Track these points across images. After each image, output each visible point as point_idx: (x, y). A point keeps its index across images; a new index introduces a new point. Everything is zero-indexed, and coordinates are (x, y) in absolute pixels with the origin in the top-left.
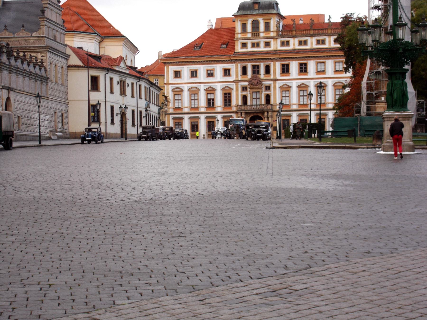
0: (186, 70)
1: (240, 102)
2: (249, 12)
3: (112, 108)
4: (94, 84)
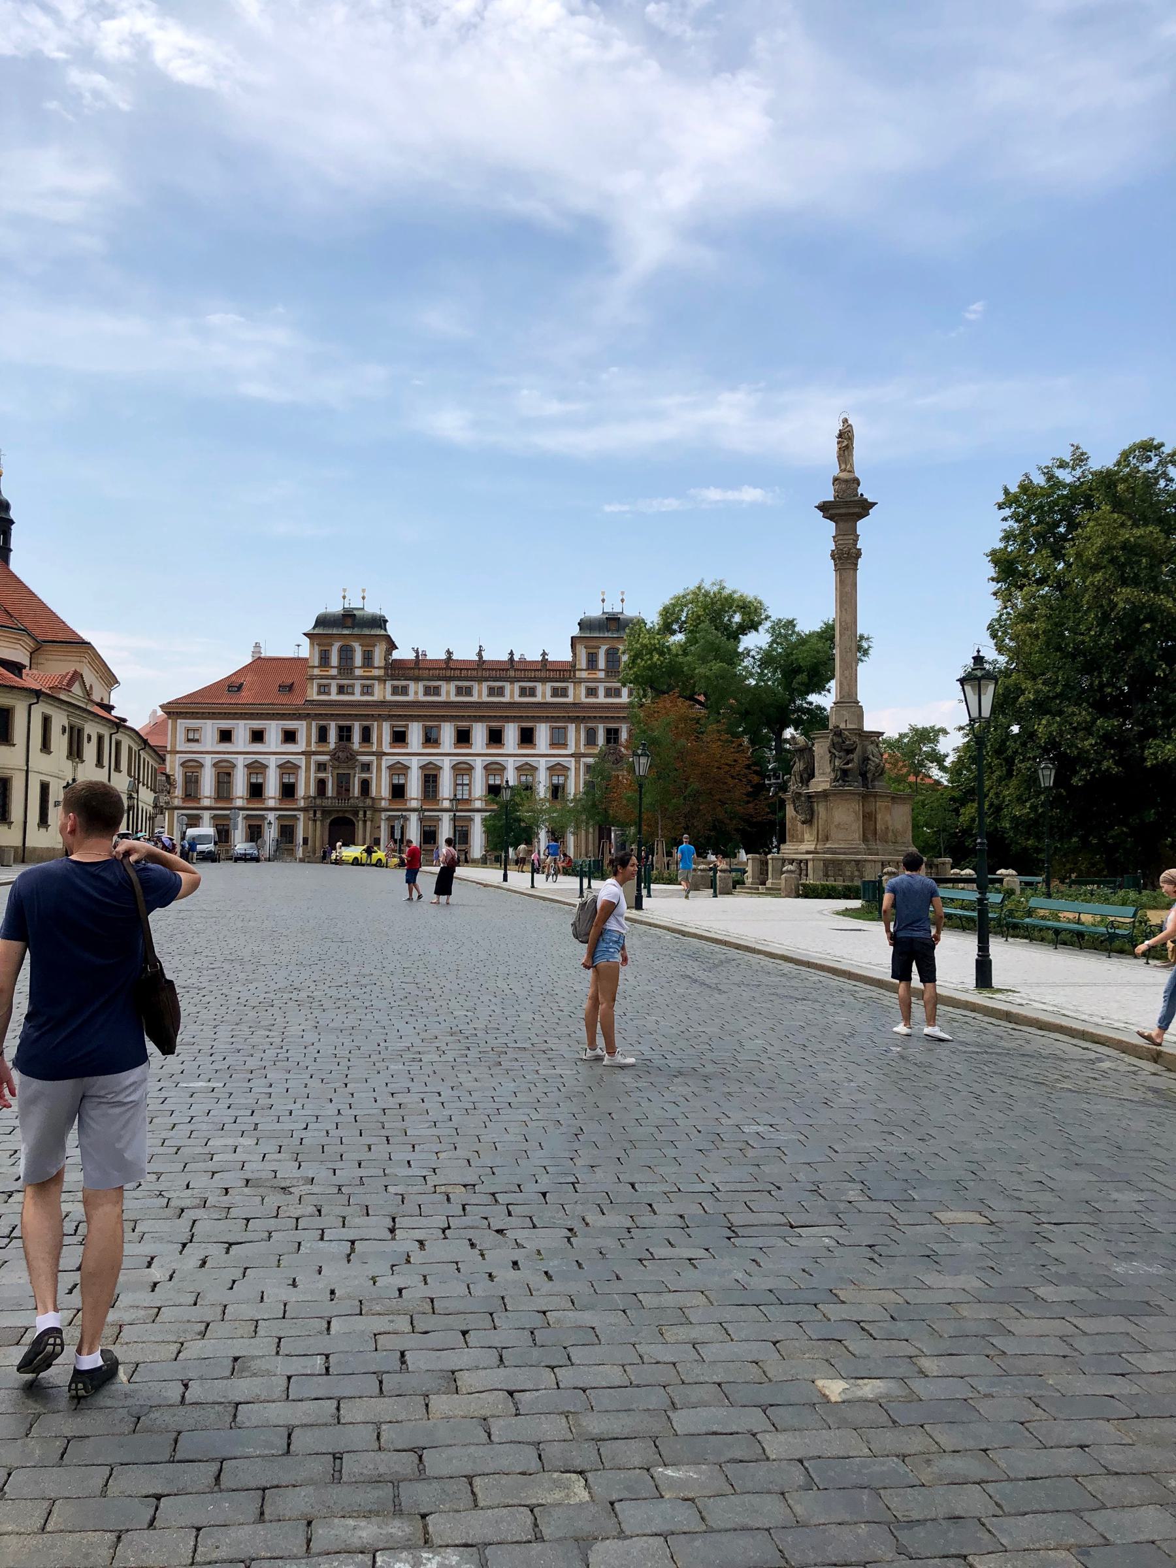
0: (209, 729)
1: (312, 792)
2: (335, 631)
3: (45, 788)
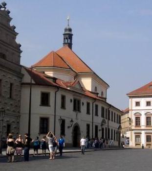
4: (45, 100)
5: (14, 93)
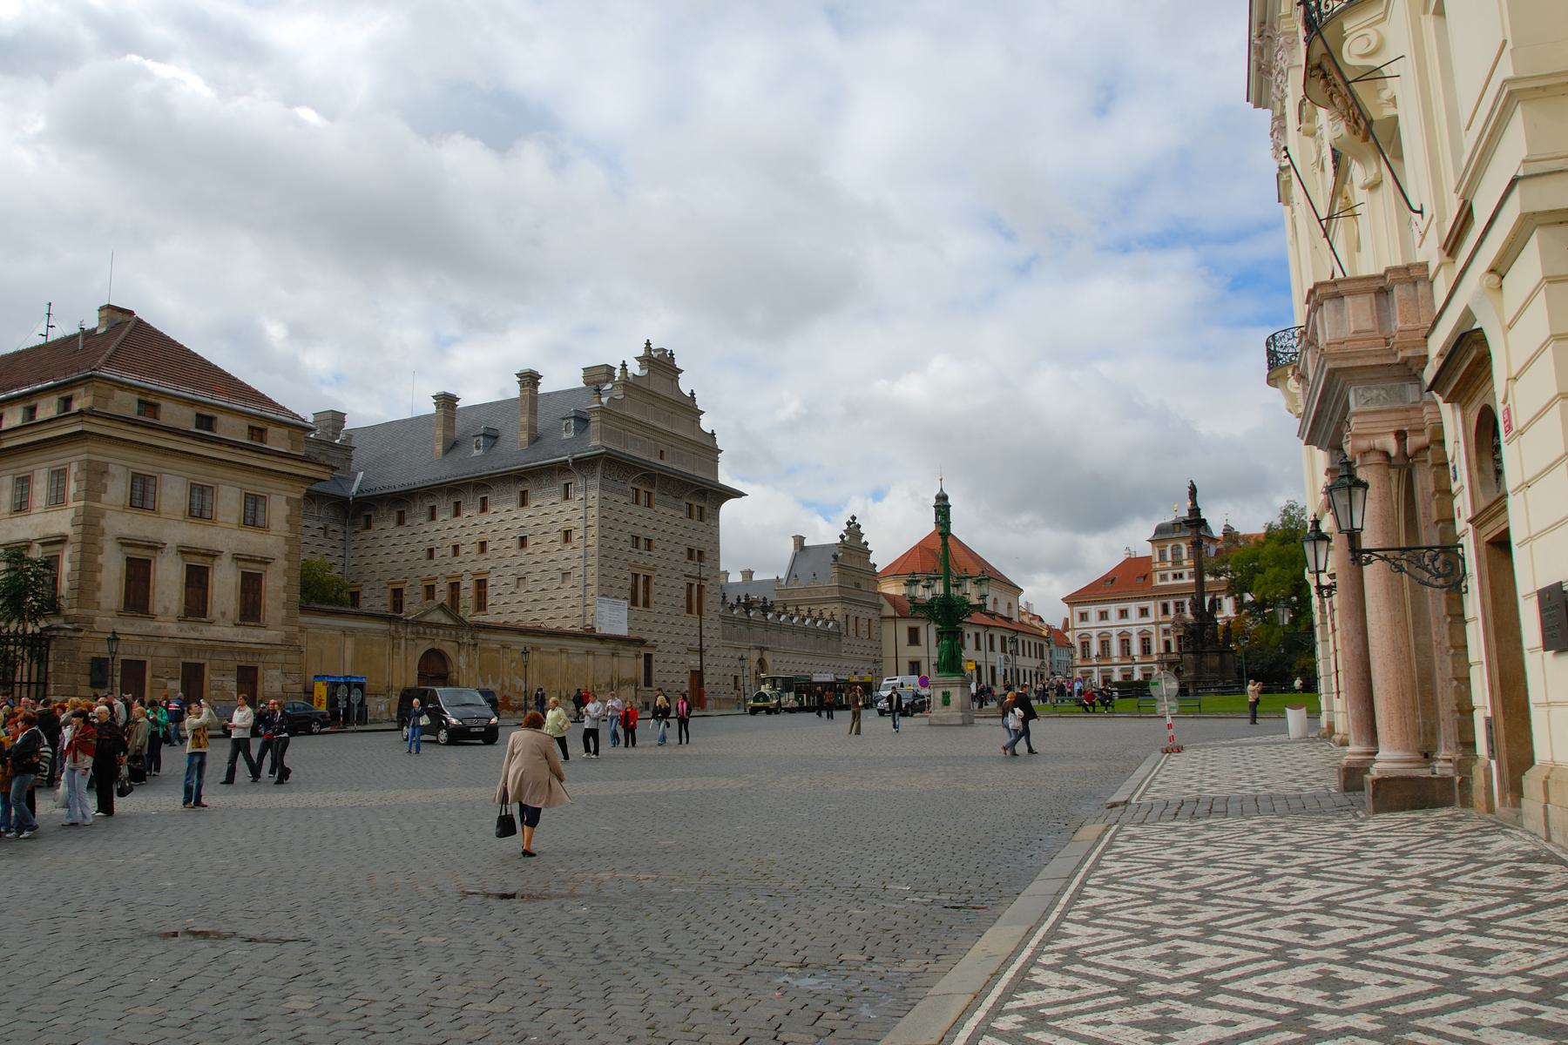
0: (1093, 611)
5: (873, 631)
